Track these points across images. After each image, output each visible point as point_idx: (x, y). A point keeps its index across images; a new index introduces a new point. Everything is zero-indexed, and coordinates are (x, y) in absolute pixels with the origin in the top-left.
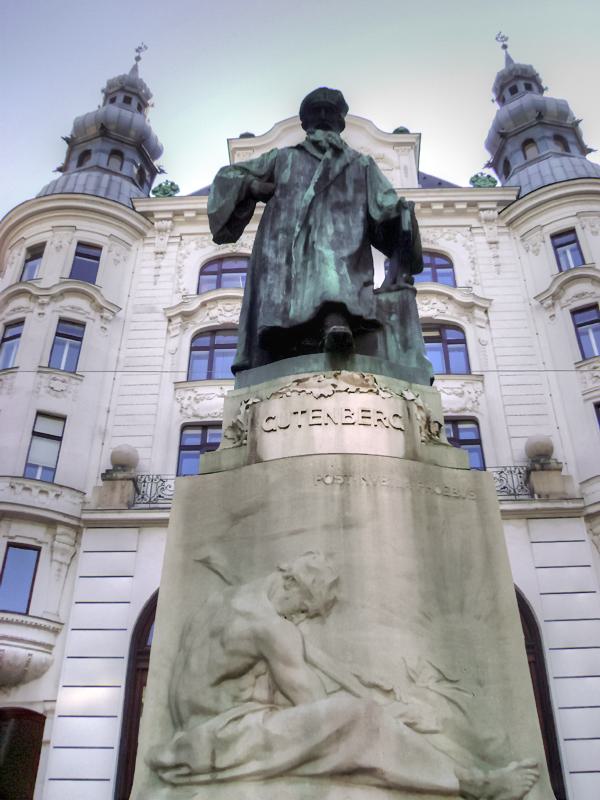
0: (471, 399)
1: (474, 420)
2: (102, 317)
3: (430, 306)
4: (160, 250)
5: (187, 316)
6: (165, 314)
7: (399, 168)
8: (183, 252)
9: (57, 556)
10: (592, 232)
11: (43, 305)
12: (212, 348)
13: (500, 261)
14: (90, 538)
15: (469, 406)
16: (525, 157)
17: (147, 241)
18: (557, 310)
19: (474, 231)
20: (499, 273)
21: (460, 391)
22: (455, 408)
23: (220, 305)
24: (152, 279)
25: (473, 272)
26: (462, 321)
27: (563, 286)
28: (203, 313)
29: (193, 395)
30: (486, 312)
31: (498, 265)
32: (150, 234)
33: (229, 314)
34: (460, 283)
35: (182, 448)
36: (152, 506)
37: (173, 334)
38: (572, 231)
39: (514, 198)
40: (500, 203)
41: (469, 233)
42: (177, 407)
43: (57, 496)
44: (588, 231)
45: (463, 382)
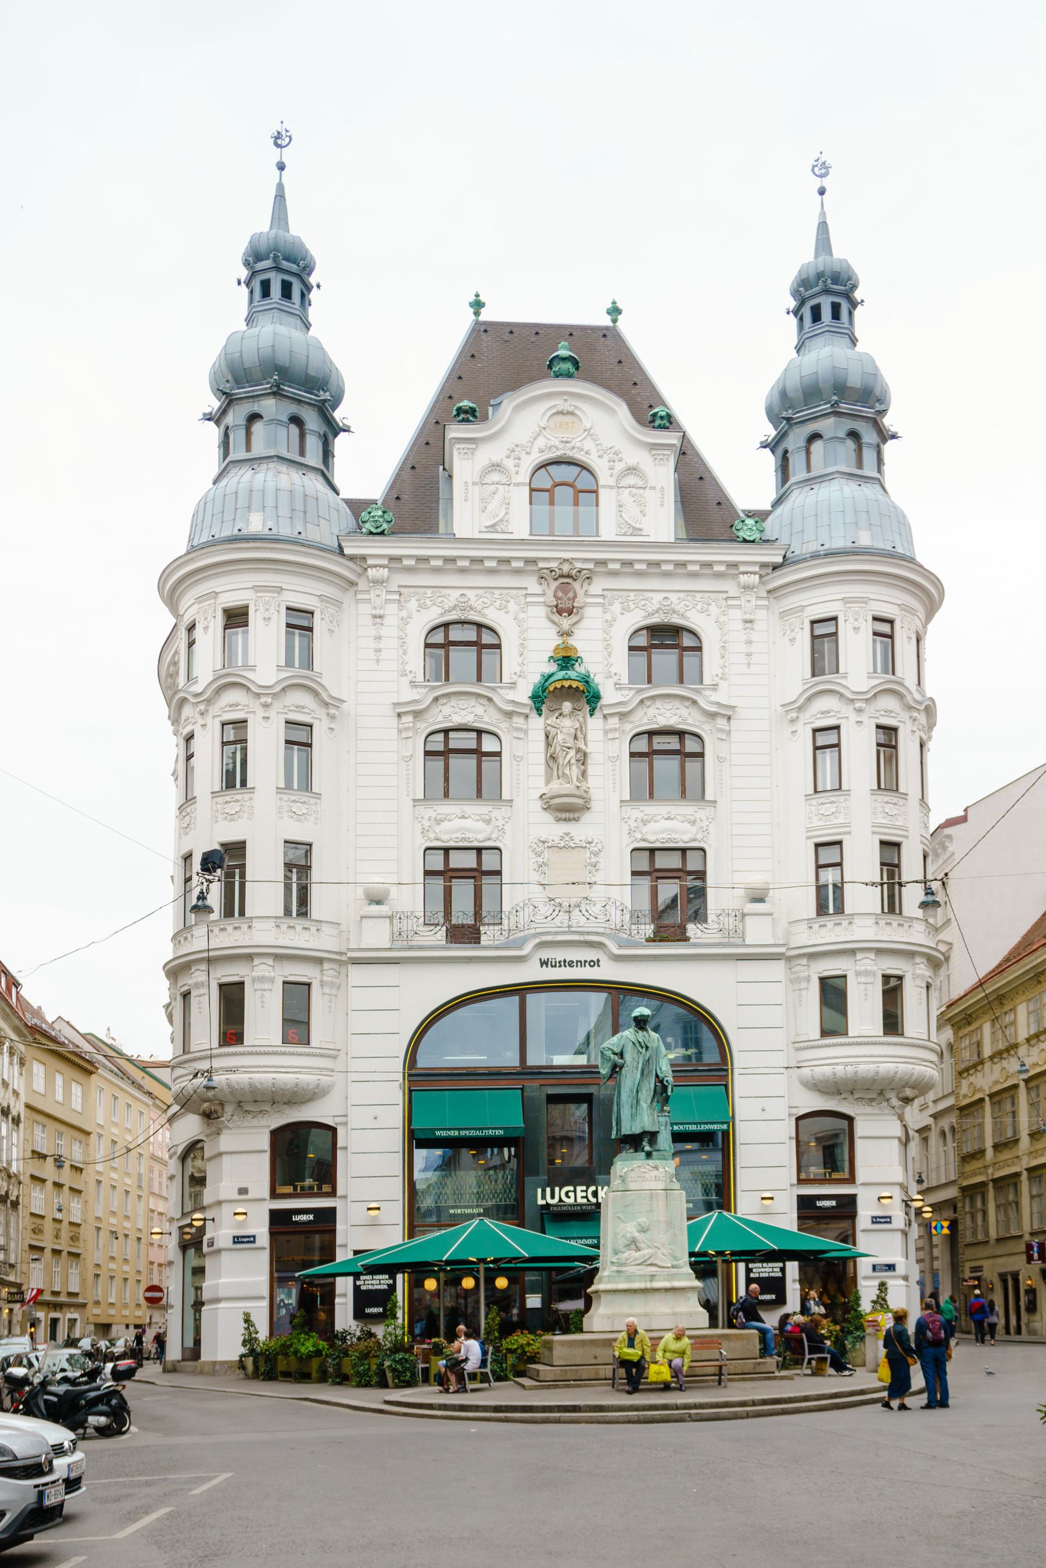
0: (702, 827)
1: (703, 850)
2: (328, 715)
3: (673, 711)
4: (378, 612)
5: (417, 714)
6: (395, 709)
7: (653, 488)
8: (404, 614)
9: (327, 990)
10: (854, 628)
11: (266, 706)
12: (446, 753)
13: (753, 648)
14: (357, 975)
15: (699, 837)
16: (809, 470)
17: (359, 596)
18: (799, 726)
19: (730, 602)
20: (749, 665)
21: (692, 818)
22: (686, 838)
23: (454, 701)
24: (372, 655)
25: (722, 662)
26: (704, 729)
27: (809, 699)
28: (435, 710)
29: (433, 815)
30: (729, 718)
31: (749, 655)
32: (362, 585)
33: (463, 713)
34: (707, 680)
35: (427, 873)
36: (410, 943)
37: (404, 735)
38: (835, 619)
39: (780, 560)
40: (763, 565)
41: (724, 603)
42: (418, 828)
43: (318, 930)
44: (849, 626)
45: (695, 808)
